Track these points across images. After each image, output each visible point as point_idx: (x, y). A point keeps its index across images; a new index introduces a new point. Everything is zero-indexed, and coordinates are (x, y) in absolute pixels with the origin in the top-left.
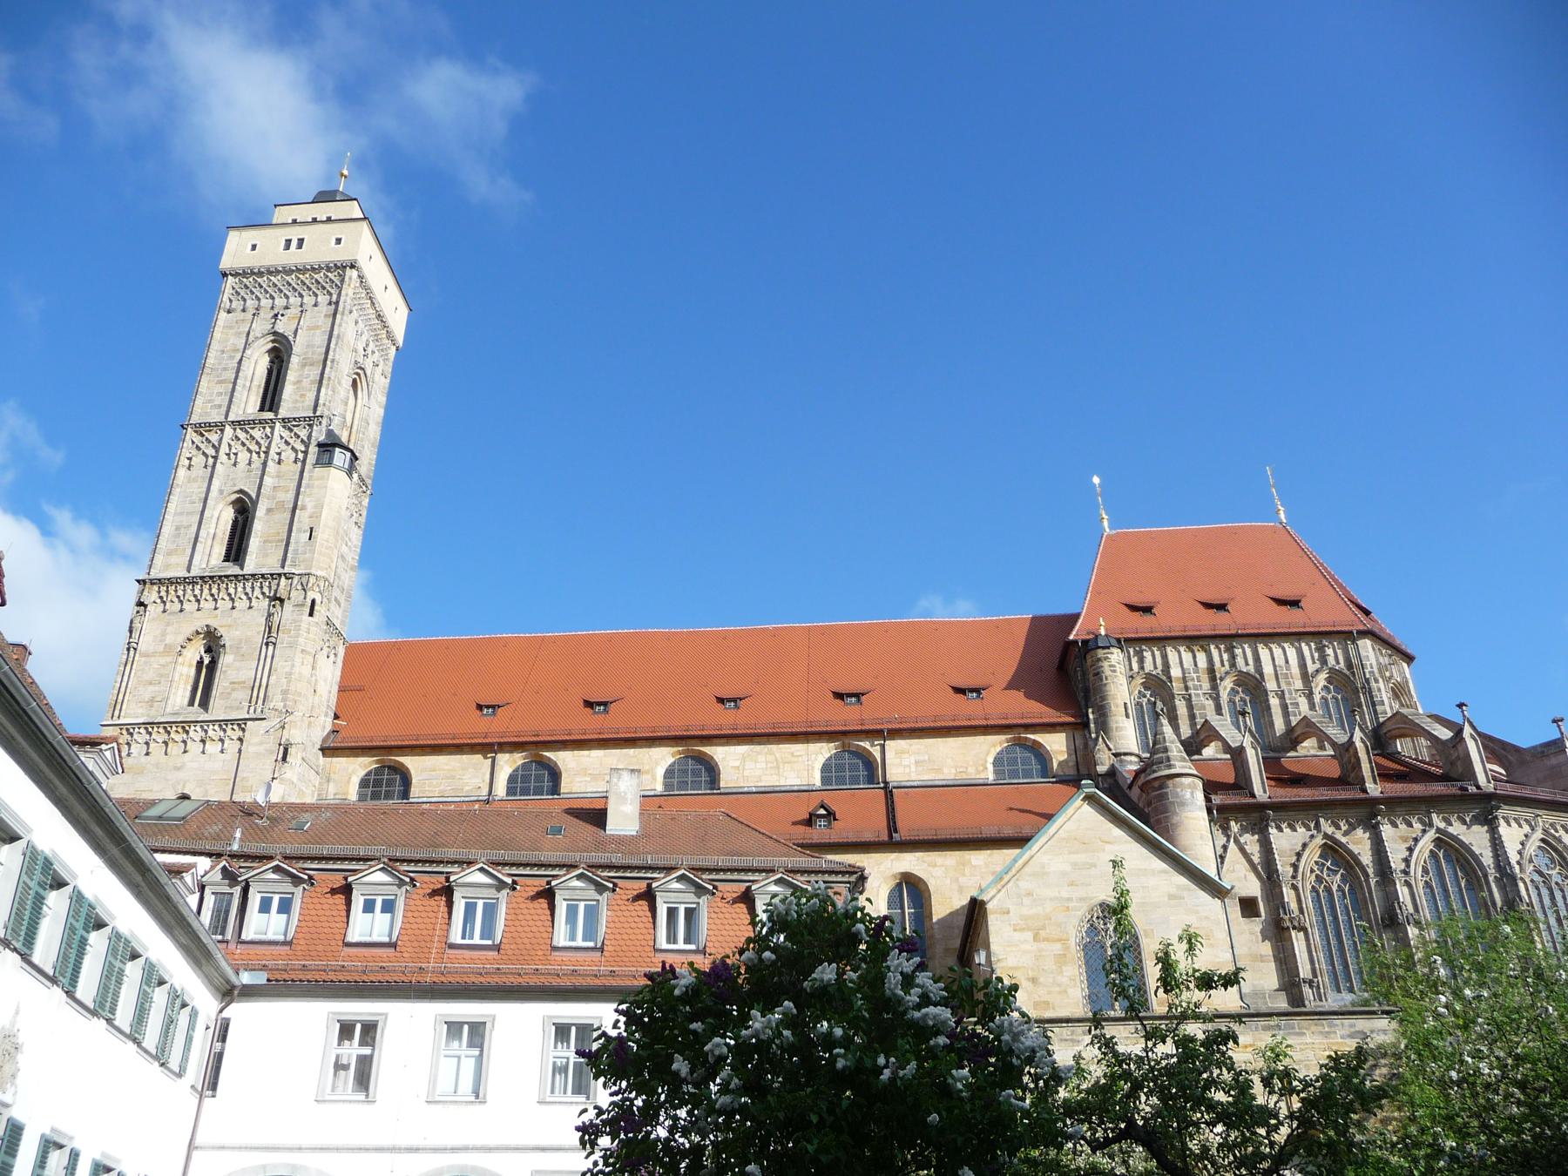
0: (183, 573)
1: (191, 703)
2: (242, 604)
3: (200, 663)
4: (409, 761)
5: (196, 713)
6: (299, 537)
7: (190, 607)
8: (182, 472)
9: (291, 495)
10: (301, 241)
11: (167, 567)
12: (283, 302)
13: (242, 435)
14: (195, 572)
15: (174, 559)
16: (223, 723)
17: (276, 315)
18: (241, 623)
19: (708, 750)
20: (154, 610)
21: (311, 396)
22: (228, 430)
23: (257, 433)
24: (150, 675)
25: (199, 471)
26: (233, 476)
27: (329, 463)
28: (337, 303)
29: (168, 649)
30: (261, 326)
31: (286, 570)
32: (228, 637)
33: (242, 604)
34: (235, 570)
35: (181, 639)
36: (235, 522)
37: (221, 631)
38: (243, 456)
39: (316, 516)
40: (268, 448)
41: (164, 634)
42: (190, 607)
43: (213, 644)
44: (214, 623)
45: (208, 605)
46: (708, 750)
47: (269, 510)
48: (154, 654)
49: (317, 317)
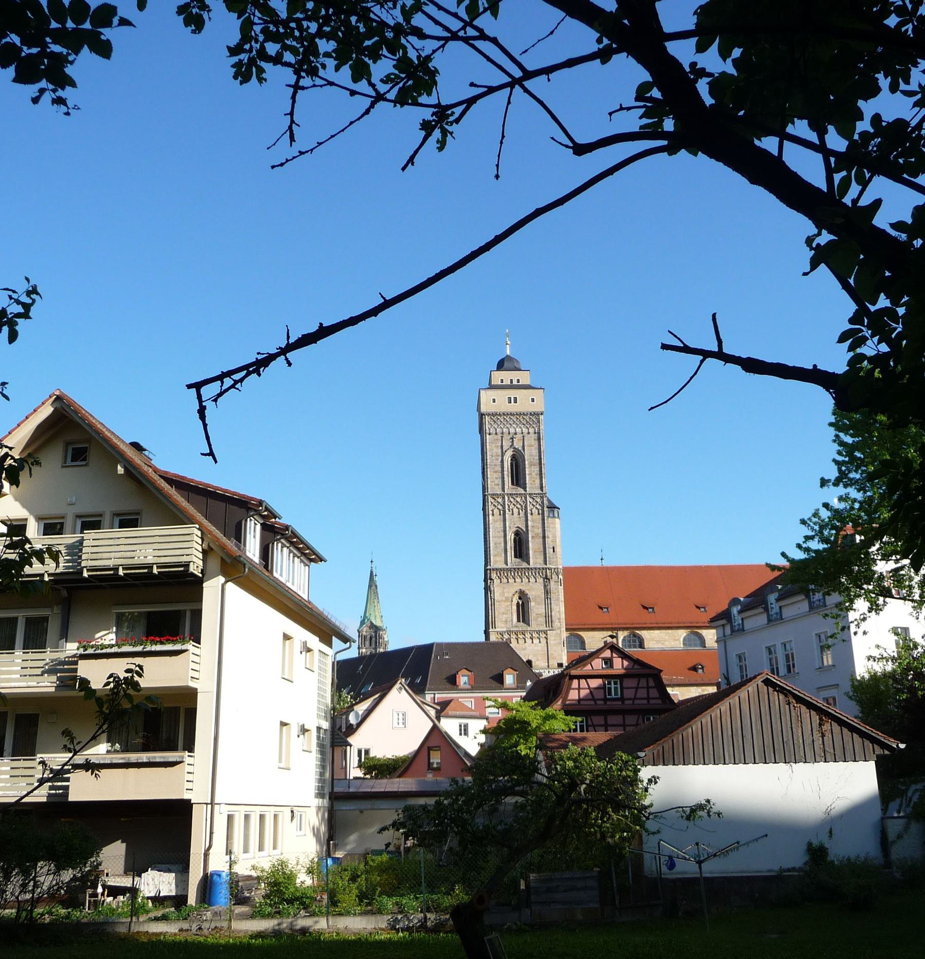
0: (504, 566)
1: (519, 620)
2: (533, 580)
3: (518, 603)
4: (581, 633)
5: (522, 626)
6: (549, 551)
7: (511, 580)
8: (491, 517)
9: (540, 530)
10: (515, 399)
11: (496, 562)
12: (512, 431)
13: (512, 500)
14: (509, 566)
15: (498, 559)
16: (538, 632)
17: (512, 438)
18: (535, 589)
19: (699, 631)
20: (497, 581)
21: (538, 481)
22: (506, 498)
23: (518, 499)
24: (502, 610)
25: (498, 517)
26: (514, 522)
27: (554, 517)
28: (539, 433)
29: (507, 599)
30: (506, 444)
31: (548, 566)
32: (531, 594)
33: (533, 580)
34: (525, 565)
35: (511, 595)
36: (515, 539)
37: (527, 592)
38: (516, 510)
39: (554, 541)
40: (526, 507)
41: (503, 593)
42: (511, 580)
43: (523, 595)
44: (523, 589)
45: (518, 580)
46: (699, 631)
47: (533, 537)
48: (501, 601)
49: (531, 440)
